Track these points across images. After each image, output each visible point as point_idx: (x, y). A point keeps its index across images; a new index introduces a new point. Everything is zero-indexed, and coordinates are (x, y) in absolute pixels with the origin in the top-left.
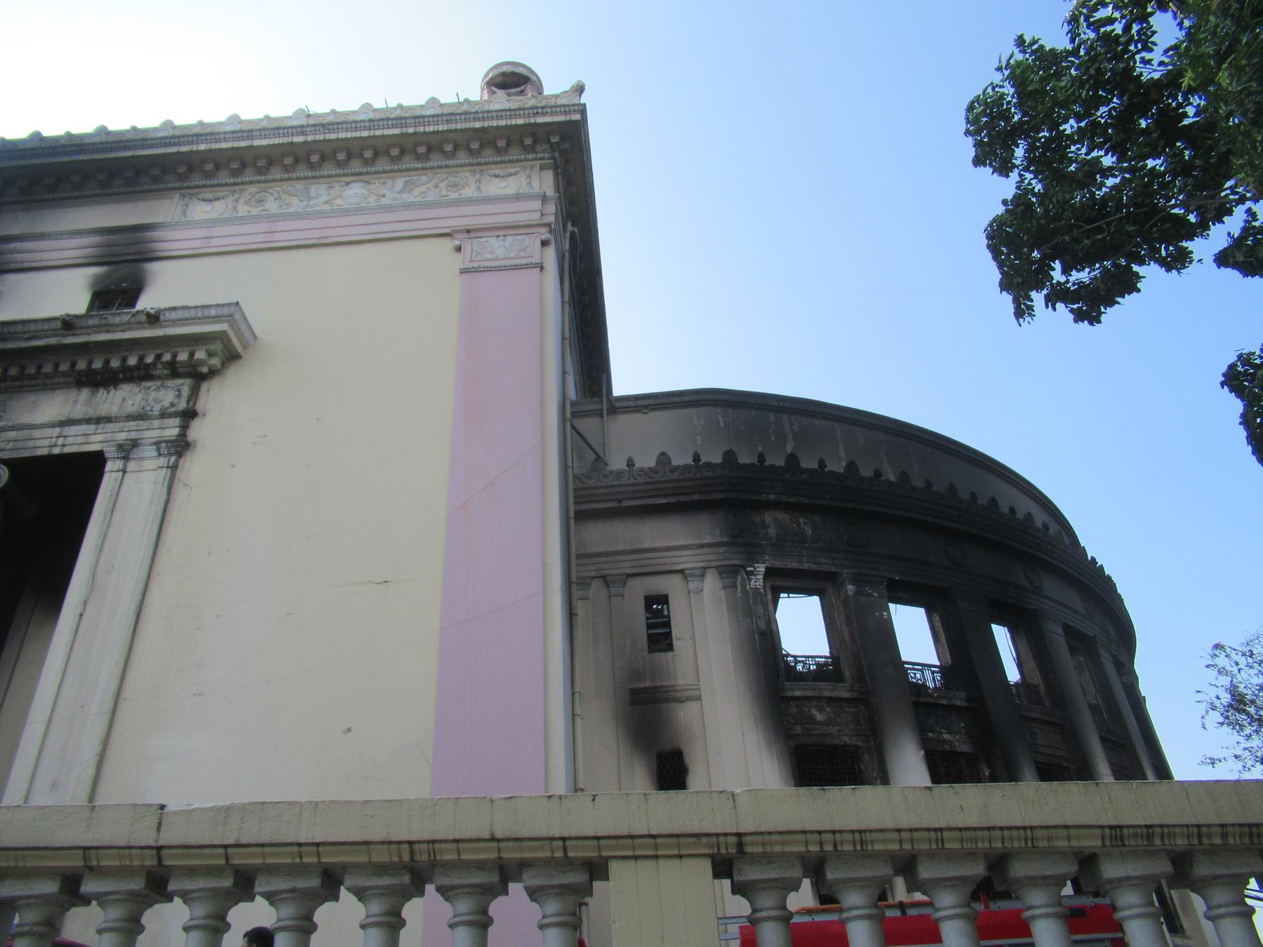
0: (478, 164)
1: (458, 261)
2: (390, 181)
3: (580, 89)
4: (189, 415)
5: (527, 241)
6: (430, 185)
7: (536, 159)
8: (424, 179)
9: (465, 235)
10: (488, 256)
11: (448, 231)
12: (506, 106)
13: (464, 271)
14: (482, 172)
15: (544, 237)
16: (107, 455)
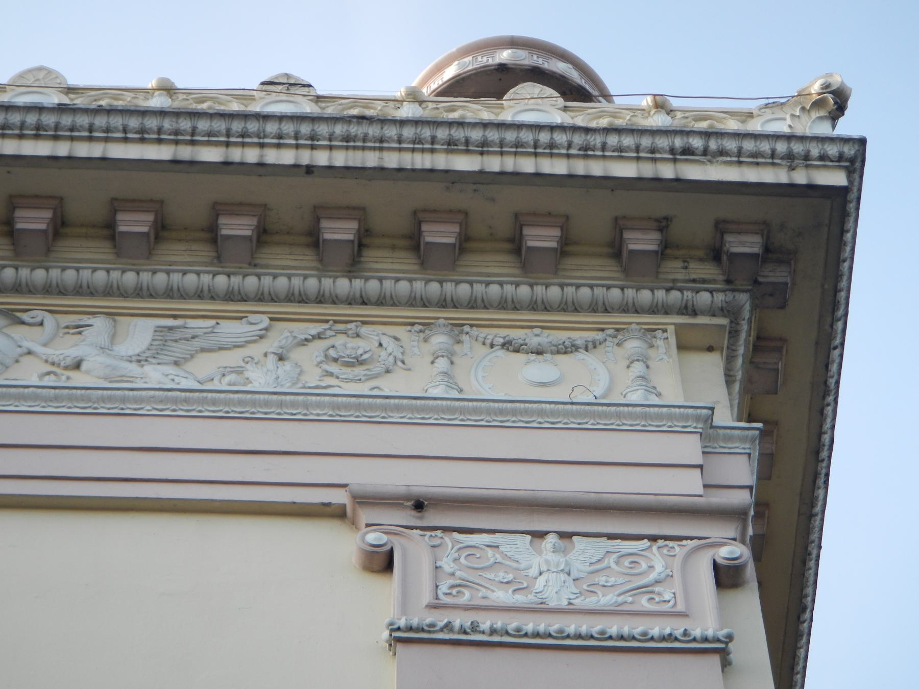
0: (444, 303)
1: (382, 604)
2: (100, 323)
3: (836, 102)
5: (657, 561)
6: (256, 350)
7: (654, 310)
8: (231, 329)
9: (406, 517)
10: (502, 596)
11: (339, 497)
12: (558, 118)
13: (404, 637)
14: (457, 326)
15: (724, 553)
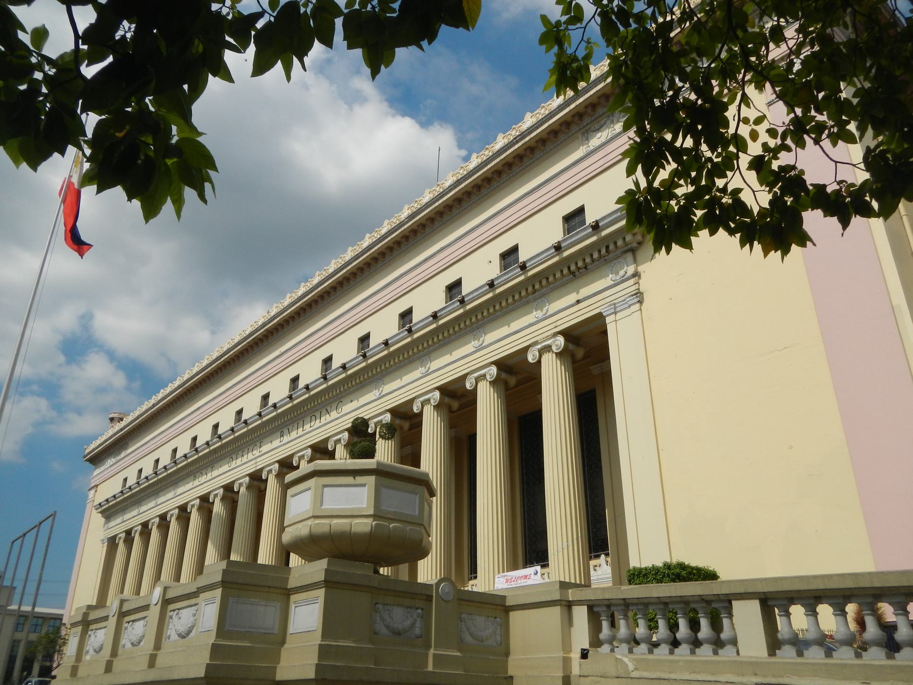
4: (636, 275)
16: (604, 314)
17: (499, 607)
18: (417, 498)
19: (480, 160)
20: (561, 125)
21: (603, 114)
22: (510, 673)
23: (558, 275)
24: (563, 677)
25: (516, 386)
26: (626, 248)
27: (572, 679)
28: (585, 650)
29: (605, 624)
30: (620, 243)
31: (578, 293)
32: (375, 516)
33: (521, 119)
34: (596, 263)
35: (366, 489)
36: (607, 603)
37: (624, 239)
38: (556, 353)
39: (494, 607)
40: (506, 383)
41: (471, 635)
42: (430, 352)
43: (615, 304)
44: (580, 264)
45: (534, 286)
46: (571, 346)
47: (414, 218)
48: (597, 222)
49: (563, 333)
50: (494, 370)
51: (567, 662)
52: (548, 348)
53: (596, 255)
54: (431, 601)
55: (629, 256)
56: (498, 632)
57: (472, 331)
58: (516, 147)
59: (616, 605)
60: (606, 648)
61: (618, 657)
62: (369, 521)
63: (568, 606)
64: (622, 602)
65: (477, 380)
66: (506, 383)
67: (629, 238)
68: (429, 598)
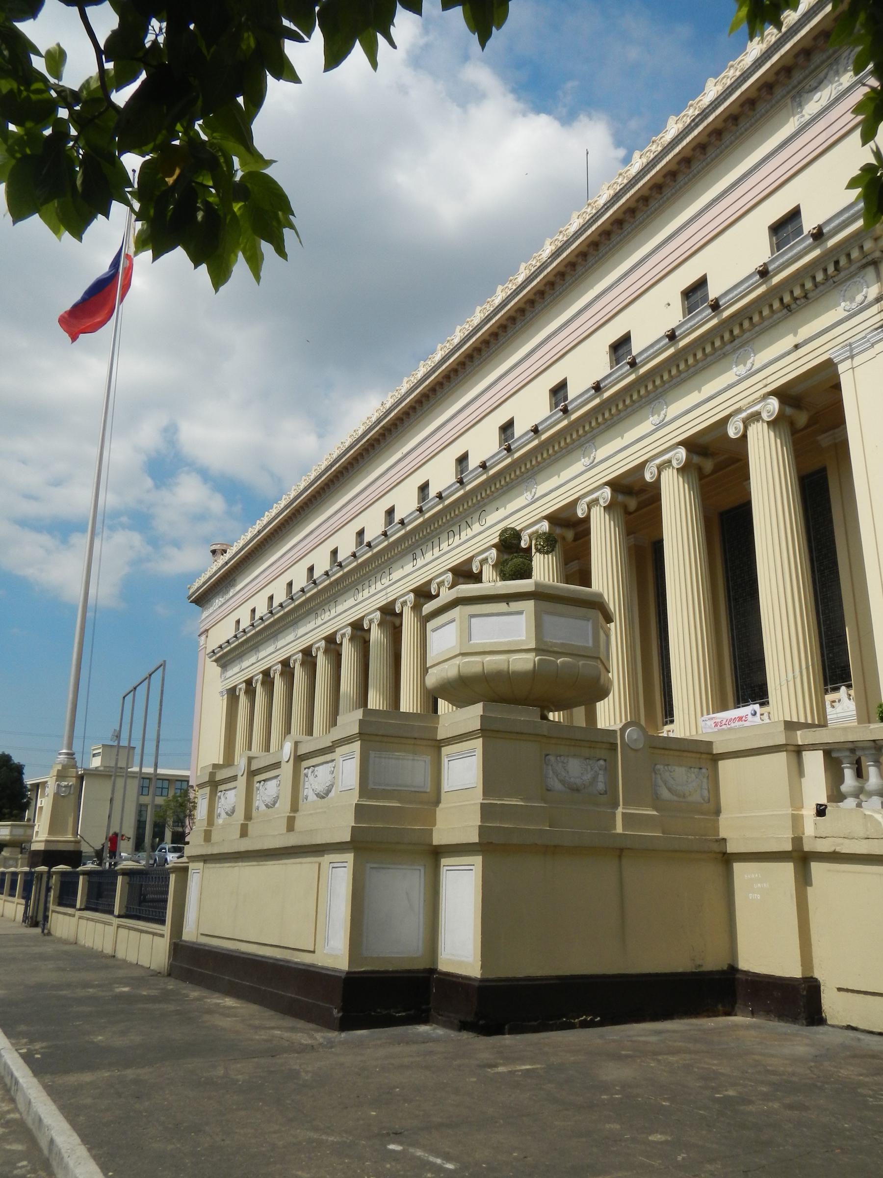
16: (836, 361)
17: (704, 756)
18: (590, 625)
19: (645, 161)
20: (759, 89)
21: (823, 62)
22: (722, 834)
23: (766, 312)
24: (793, 839)
25: (714, 472)
26: (864, 261)
27: (805, 841)
28: (821, 805)
29: (849, 774)
30: (855, 254)
31: (795, 334)
32: (537, 650)
33: (700, 89)
34: (821, 288)
35: (523, 617)
36: (851, 746)
37: (862, 247)
38: (768, 423)
39: (698, 756)
40: (700, 469)
41: (669, 789)
42: (594, 437)
43: (850, 344)
44: (797, 292)
45: (731, 332)
46: (789, 411)
47: (559, 255)
48: (820, 228)
49: (775, 393)
50: (682, 452)
51: (797, 821)
52: (756, 417)
53: (820, 277)
54: (616, 750)
55: (870, 272)
56: (705, 786)
57: (650, 402)
58: (696, 132)
59: (863, 749)
60: (850, 803)
61: (868, 813)
62: (531, 656)
63: (798, 751)
64: (872, 744)
65: (660, 469)
66: (700, 469)
67: (868, 245)
68: (613, 747)
